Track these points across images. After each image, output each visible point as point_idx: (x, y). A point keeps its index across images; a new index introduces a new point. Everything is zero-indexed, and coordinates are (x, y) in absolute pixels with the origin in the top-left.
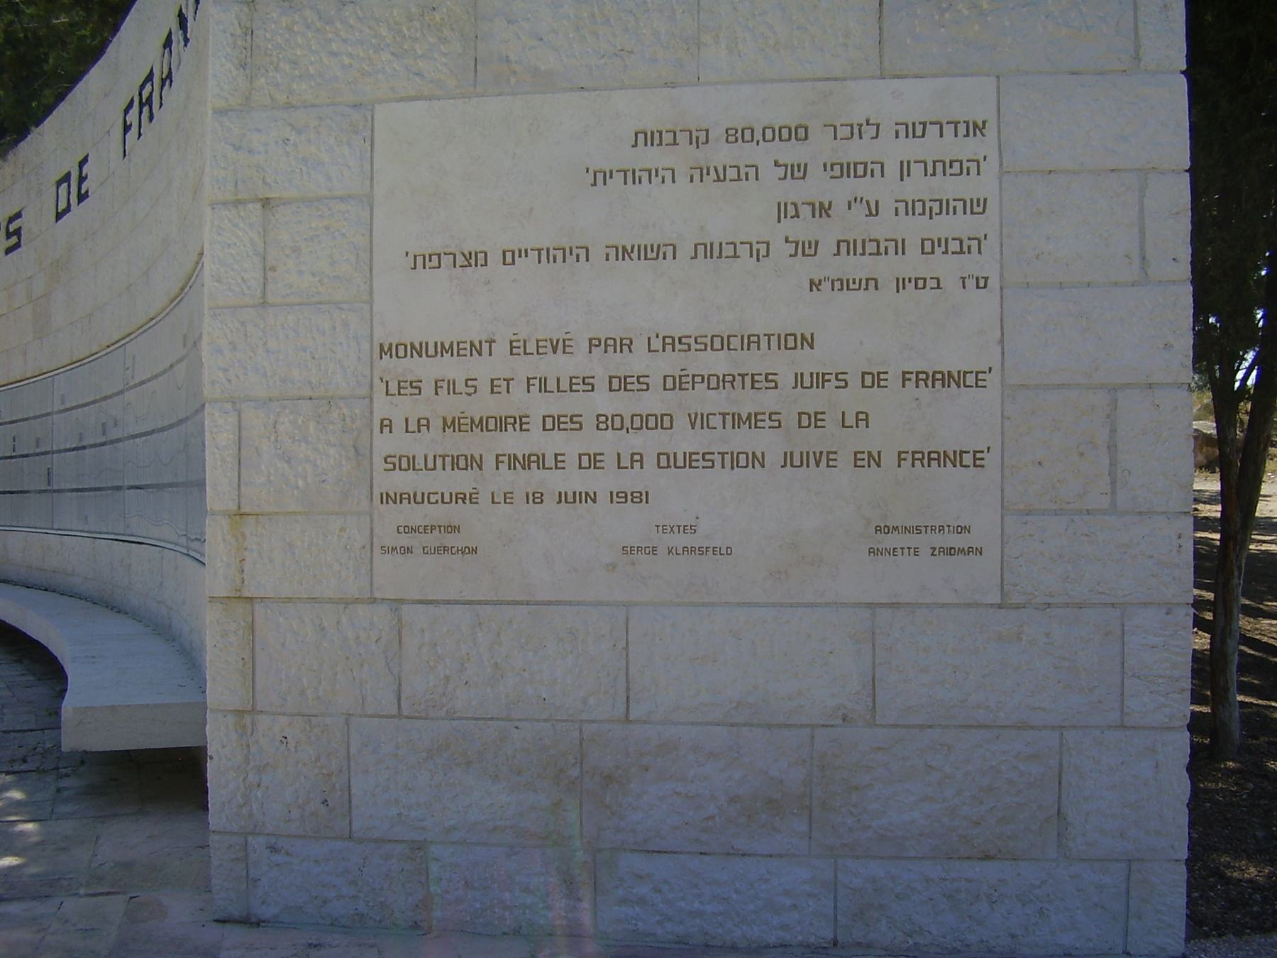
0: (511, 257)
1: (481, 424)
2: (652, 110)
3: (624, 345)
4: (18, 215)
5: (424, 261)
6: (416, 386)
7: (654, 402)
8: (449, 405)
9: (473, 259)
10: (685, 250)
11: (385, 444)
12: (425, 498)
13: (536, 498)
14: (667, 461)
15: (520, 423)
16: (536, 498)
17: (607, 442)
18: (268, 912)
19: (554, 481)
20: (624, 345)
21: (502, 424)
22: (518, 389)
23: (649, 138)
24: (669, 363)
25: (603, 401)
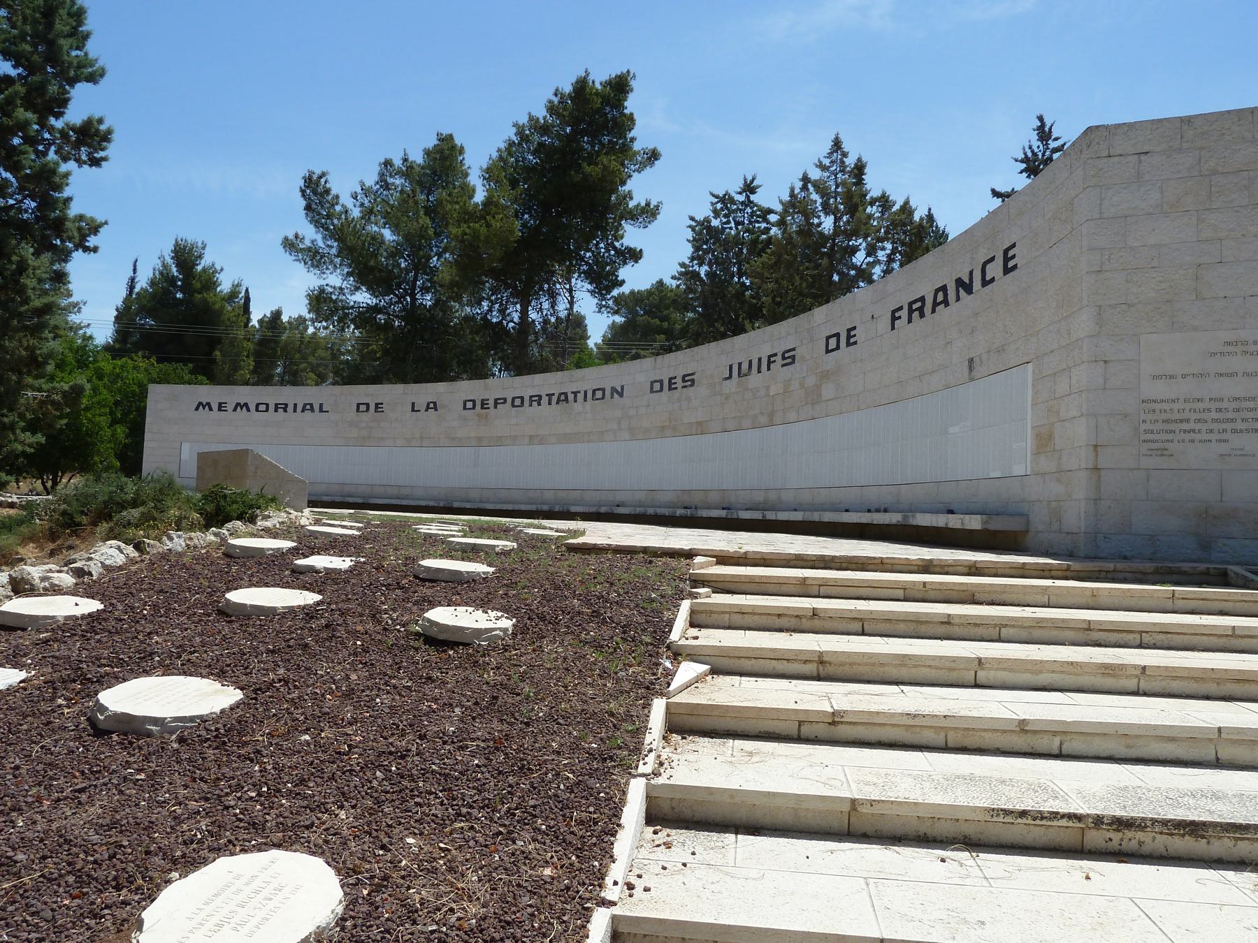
0: (1184, 376)
1: (1176, 421)
2: (1231, 336)
3: (1221, 400)
4: (794, 349)
5: (1155, 377)
6: (1154, 411)
7: (1230, 415)
8: (1164, 416)
9: (1171, 377)
10: (1240, 374)
11: (1143, 427)
12: (1156, 441)
13: (1193, 441)
14: (1234, 431)
15: (1188, 421)
16: (1193, 441)
17: (1215, 426)
18: (1102, 555)
19: (1198, 437)
20: (1221, 400)
21: (1181, 421)
22: (1187, 411)
23: (1229, 344)
24: (1234, 405)
25: (1214, 415)
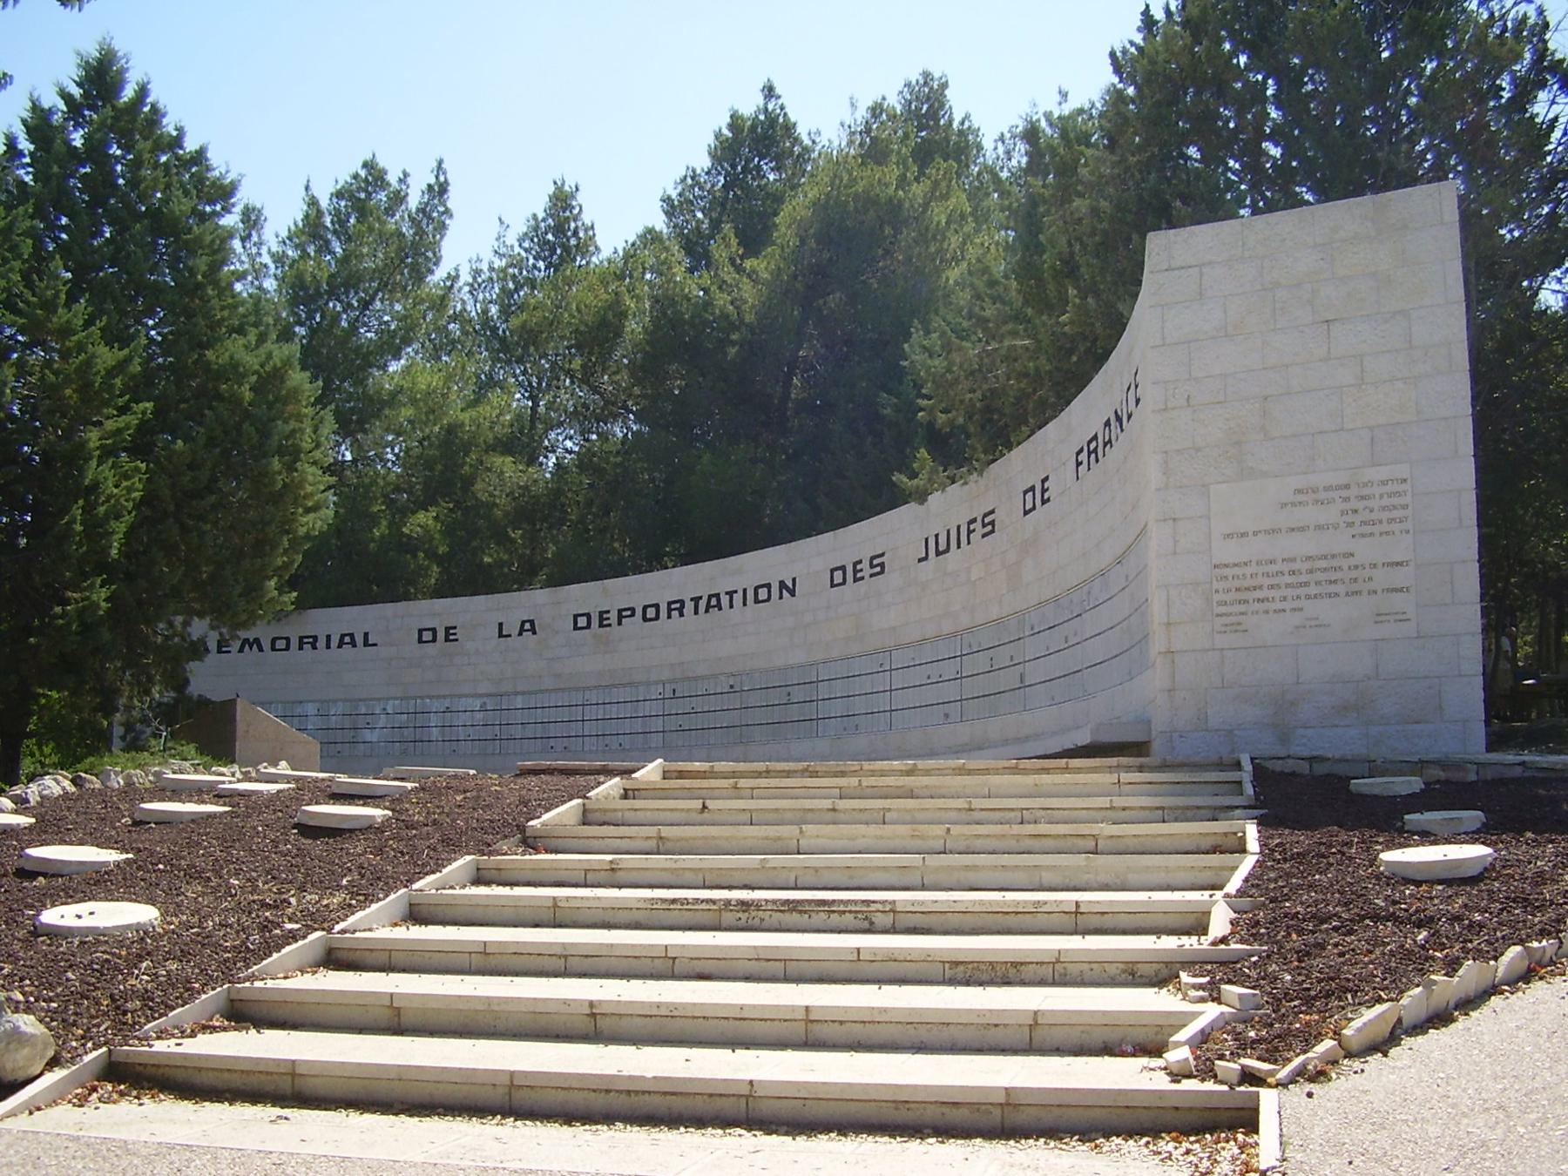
0: (1255, 533)
1: (1247, 589)
7: (1303, 578)
8: (1237, 583)
11: (1216, 597)
13: (1267, 612)
14: (1308, 597)
15: (1261, 587)
16: (1267, 612)
17: (1289, 592)
20: (1293, 560)
25: (1288, 579)
